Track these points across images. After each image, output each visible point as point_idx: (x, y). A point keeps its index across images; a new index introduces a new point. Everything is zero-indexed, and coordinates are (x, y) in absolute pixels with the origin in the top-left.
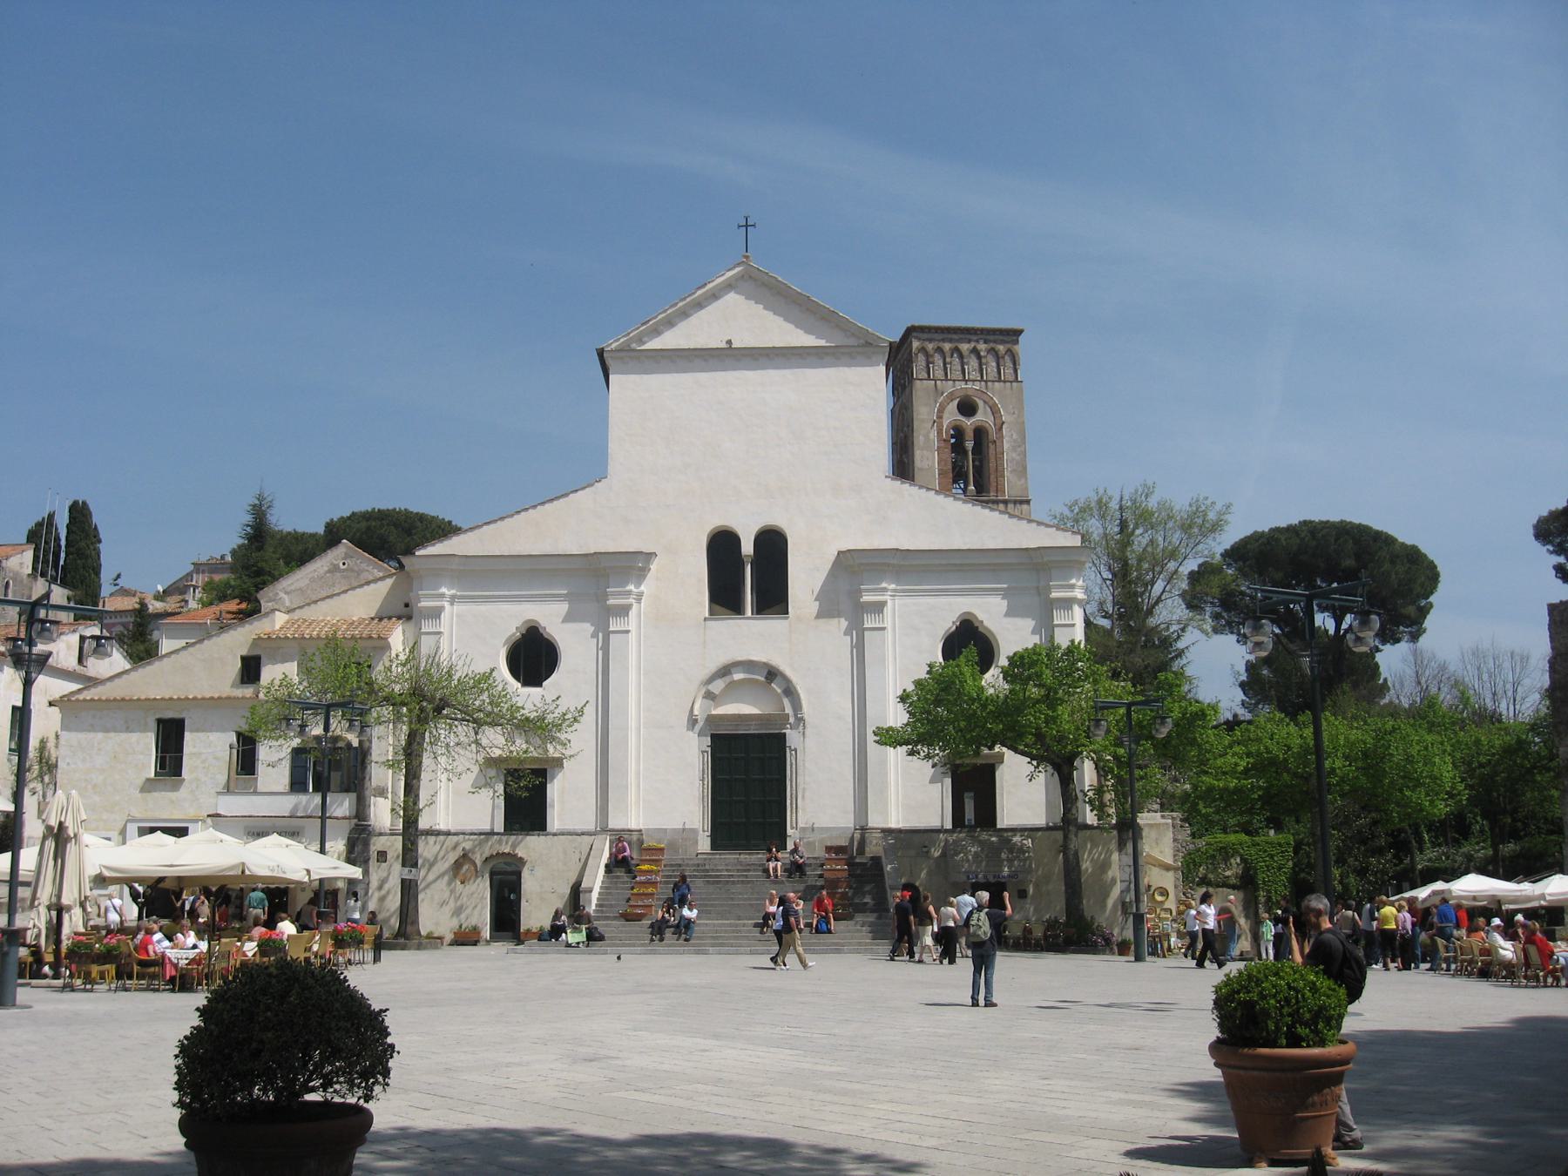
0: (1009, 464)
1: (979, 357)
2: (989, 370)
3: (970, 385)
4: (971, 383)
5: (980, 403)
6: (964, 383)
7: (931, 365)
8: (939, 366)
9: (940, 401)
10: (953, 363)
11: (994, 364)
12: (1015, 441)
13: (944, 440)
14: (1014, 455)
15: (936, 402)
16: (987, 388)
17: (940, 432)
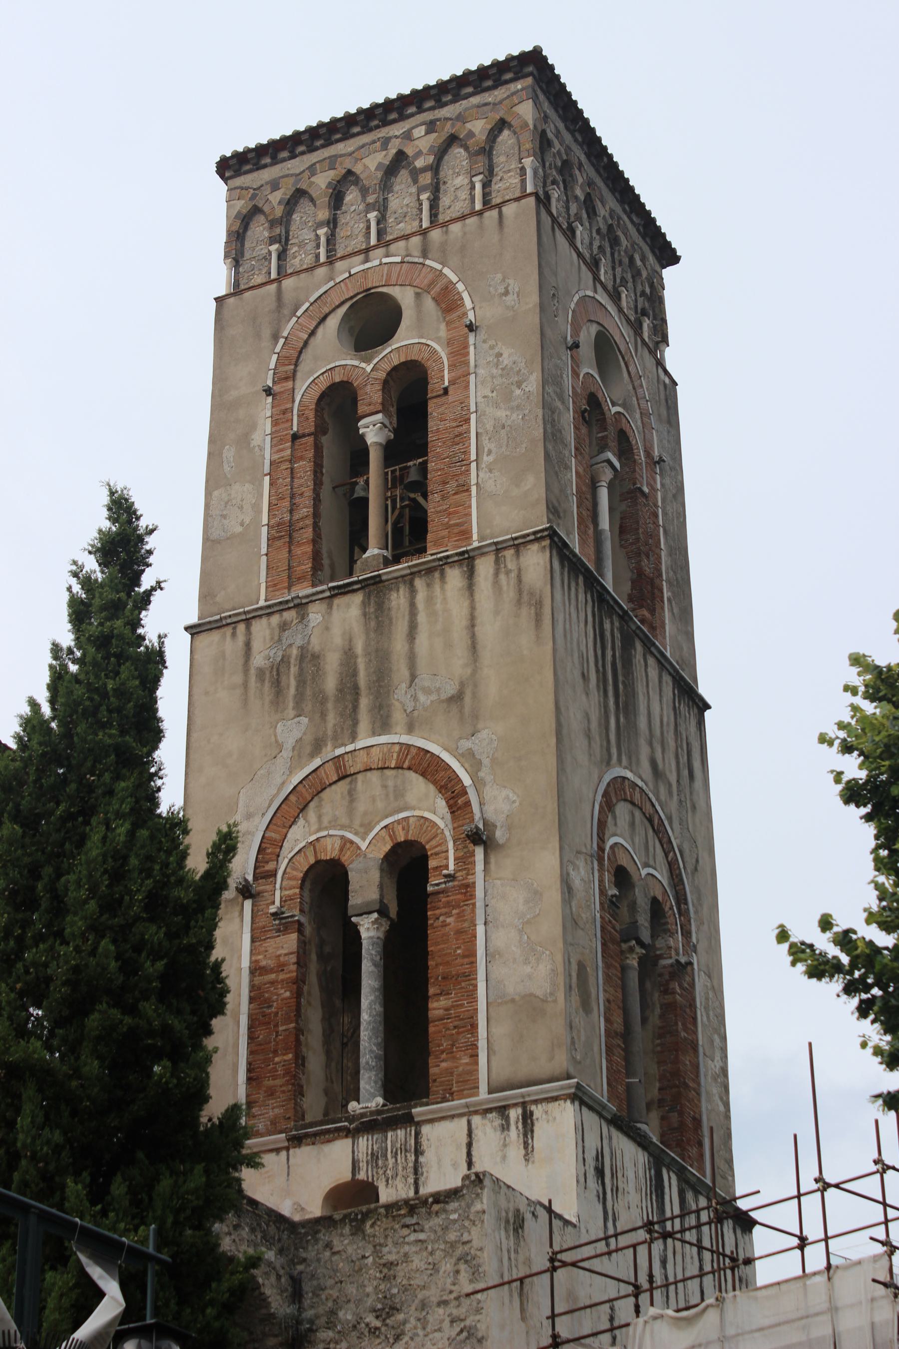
0: (487, 445)
1: (415, 174)
2: (445, 201)
3: (377, 258)
4: (380, 251)
5: (404, 297)
6: (361, 257)
7: (274, 248)
8: (302, 245)
9: (285, 334)
10: (342, 220)
11: (461, 180)
12: (506, 372)
13: (295, 437)
14: (501, 414)
15: (275, 337)
16: (425, 254)
17: (280, 418)
